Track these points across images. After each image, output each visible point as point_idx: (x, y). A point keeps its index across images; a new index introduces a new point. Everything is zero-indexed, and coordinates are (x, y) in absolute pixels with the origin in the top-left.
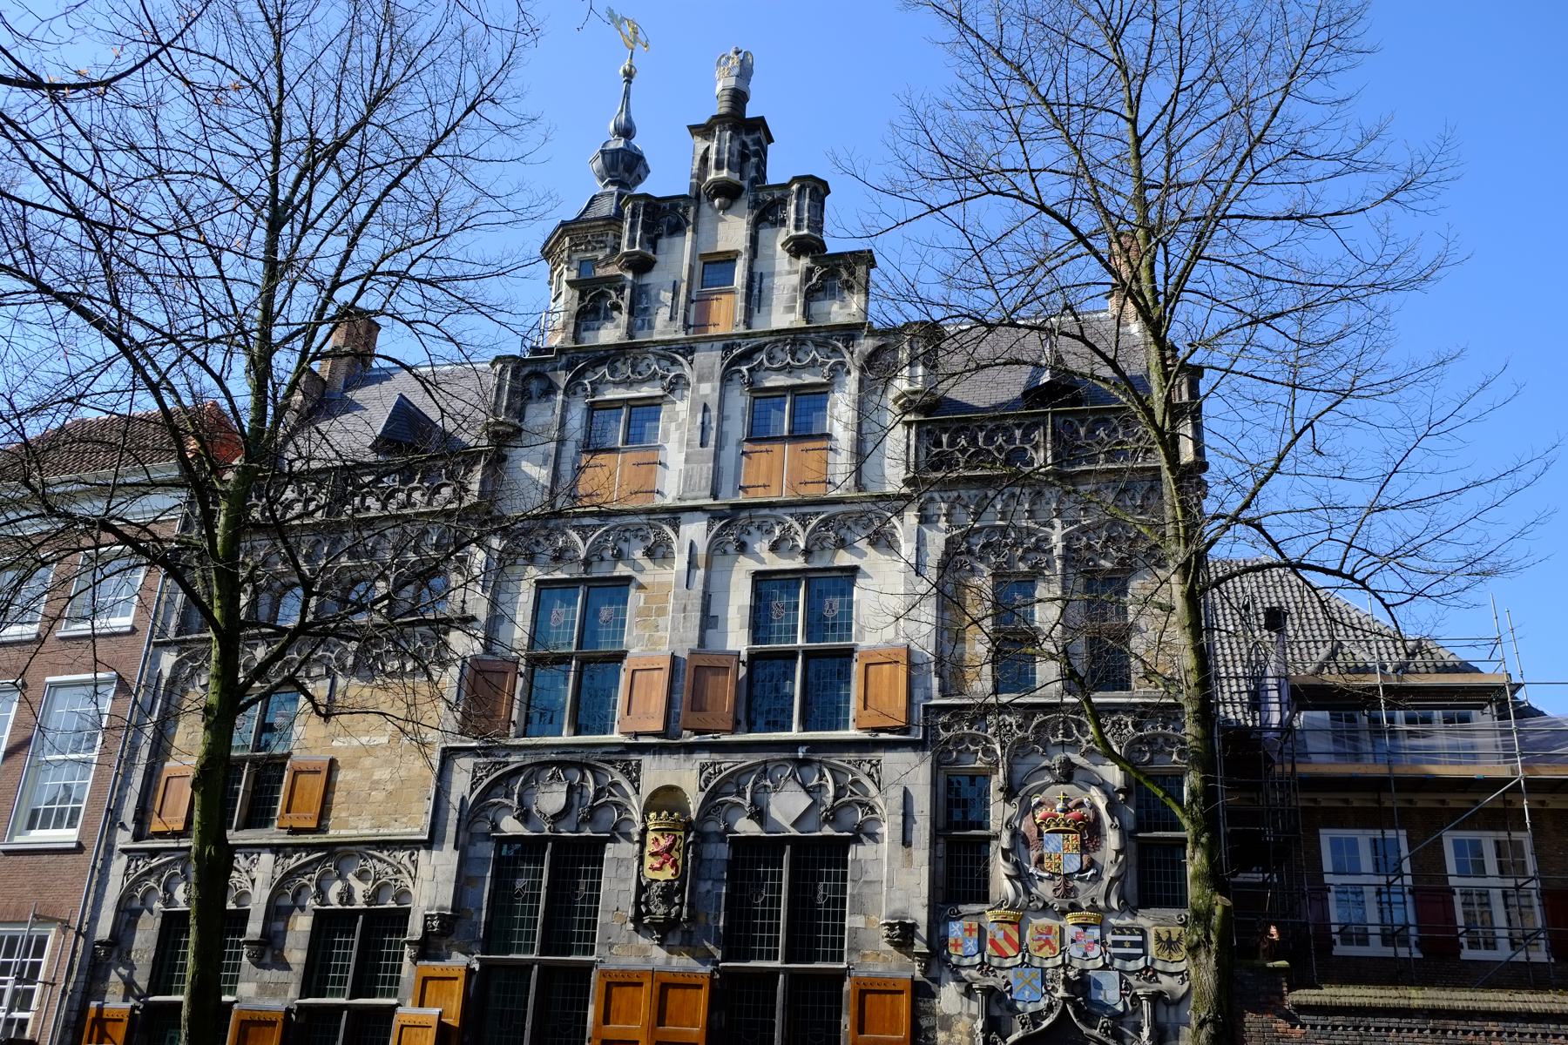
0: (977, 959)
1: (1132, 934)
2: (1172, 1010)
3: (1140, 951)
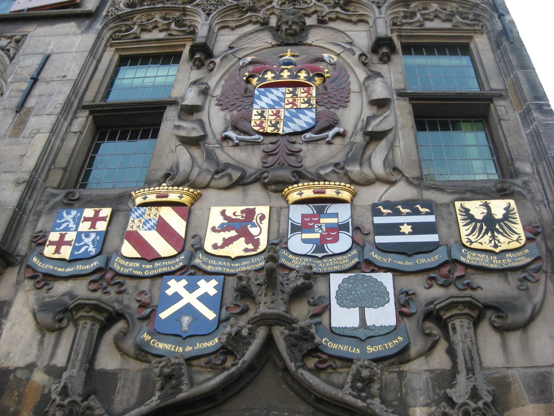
0: (95, 264)
1: (416, 212)
2: (514, 338)
3: (433, 238)
